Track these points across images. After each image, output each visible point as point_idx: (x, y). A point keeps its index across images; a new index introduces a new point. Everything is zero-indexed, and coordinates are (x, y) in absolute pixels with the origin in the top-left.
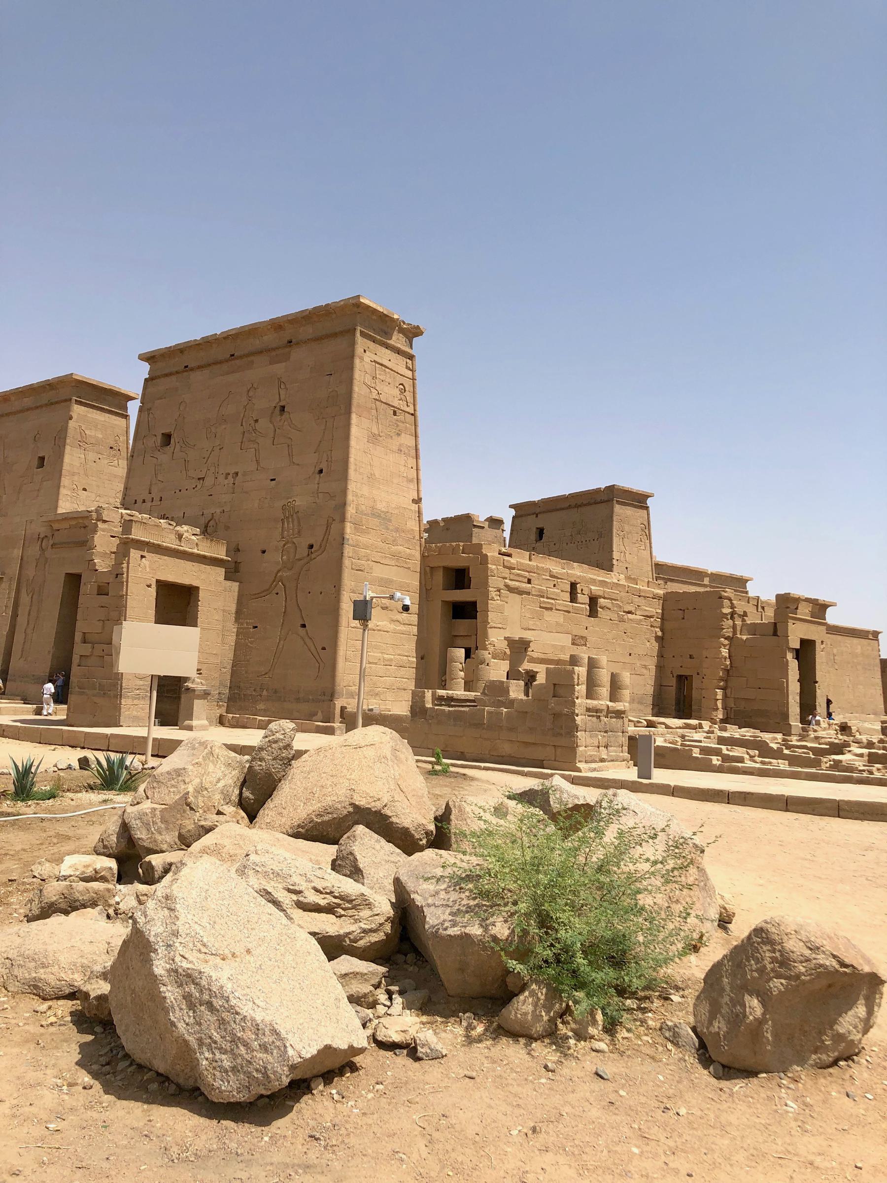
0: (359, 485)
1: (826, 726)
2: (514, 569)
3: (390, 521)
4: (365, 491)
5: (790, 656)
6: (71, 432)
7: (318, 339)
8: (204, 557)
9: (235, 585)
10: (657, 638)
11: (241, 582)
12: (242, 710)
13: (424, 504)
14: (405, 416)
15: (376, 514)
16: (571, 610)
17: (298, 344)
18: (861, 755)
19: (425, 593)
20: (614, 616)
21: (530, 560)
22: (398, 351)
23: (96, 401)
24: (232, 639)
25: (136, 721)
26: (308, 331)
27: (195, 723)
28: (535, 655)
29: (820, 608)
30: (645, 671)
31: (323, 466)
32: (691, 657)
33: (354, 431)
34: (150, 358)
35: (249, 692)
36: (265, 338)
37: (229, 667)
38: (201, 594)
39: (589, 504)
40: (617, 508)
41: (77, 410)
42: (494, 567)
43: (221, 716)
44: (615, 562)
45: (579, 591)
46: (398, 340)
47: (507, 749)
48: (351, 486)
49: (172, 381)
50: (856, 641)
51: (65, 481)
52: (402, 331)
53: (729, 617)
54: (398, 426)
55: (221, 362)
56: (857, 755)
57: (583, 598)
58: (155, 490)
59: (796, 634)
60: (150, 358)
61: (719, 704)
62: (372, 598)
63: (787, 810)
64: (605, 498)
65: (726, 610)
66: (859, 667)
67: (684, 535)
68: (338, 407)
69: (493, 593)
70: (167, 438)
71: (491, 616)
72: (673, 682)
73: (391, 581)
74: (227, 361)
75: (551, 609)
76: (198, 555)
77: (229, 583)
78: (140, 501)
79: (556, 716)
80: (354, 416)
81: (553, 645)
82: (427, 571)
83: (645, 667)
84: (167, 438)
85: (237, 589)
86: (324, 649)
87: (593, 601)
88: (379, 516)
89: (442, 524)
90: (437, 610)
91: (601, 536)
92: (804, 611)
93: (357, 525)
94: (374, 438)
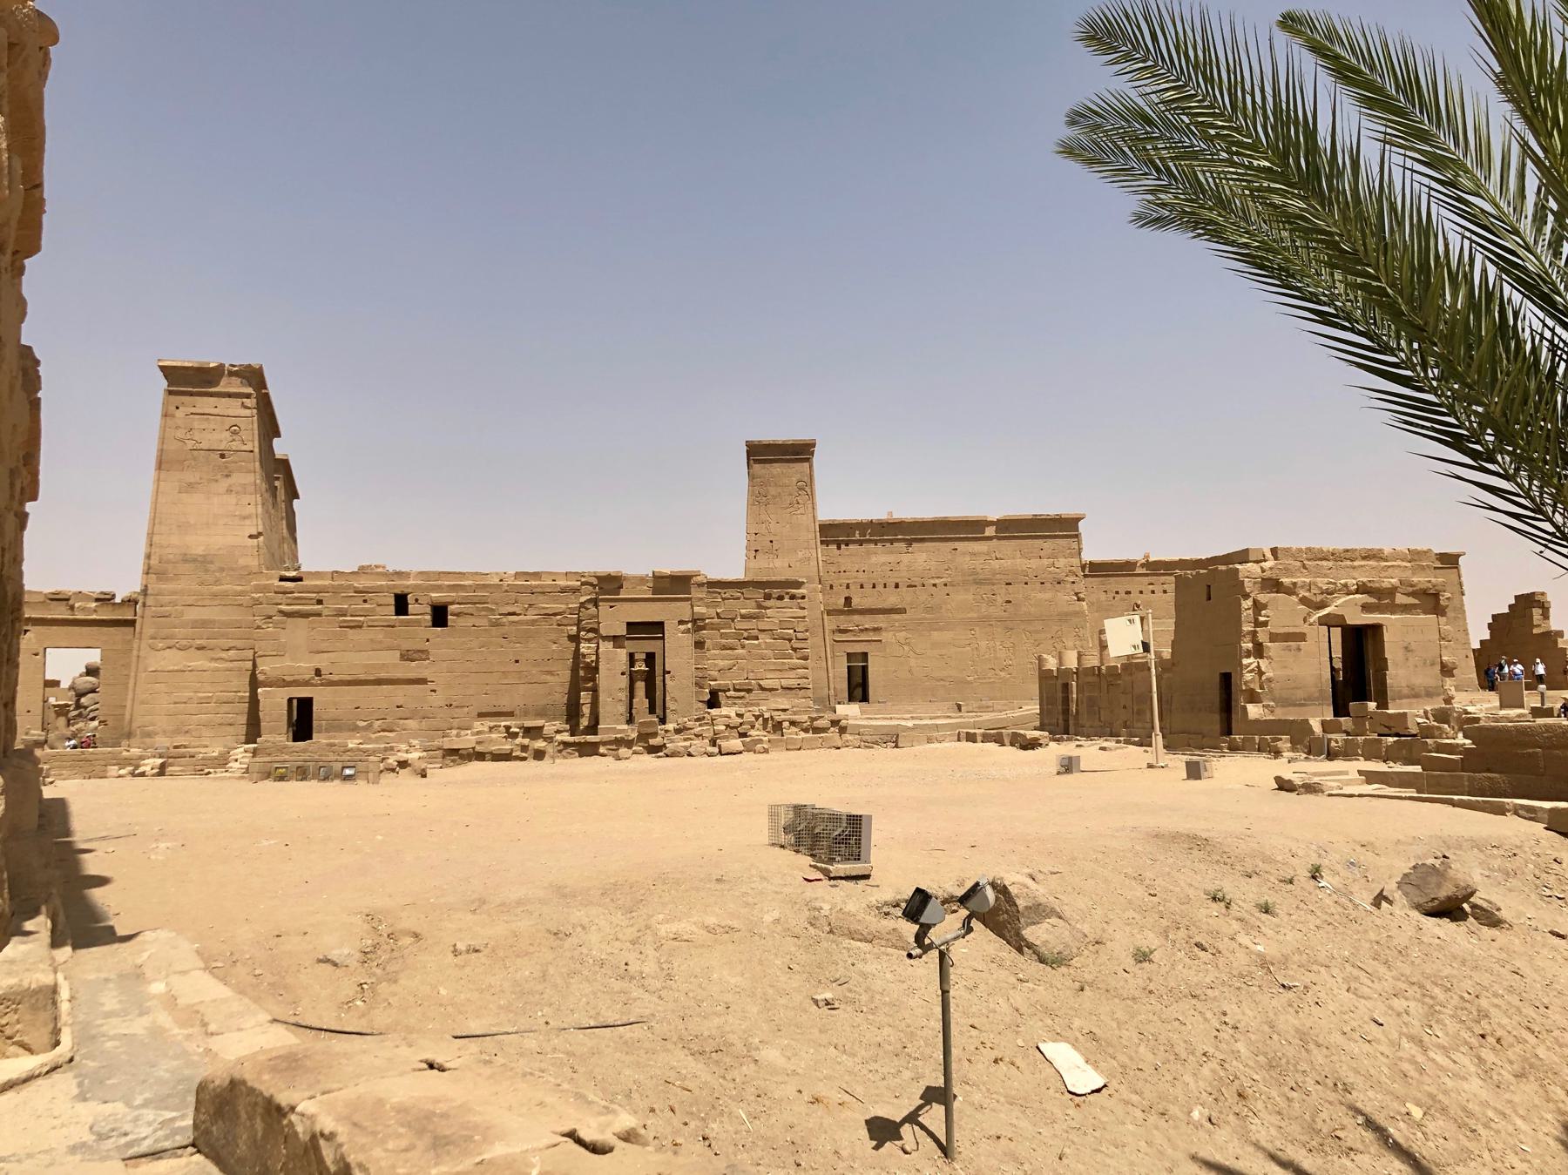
15: (186, 559)
22: (229, 395)
28: (335, 678)
30: (549, 678)
52: (231, 374)
57: (419, 611)
83: (550, 673)
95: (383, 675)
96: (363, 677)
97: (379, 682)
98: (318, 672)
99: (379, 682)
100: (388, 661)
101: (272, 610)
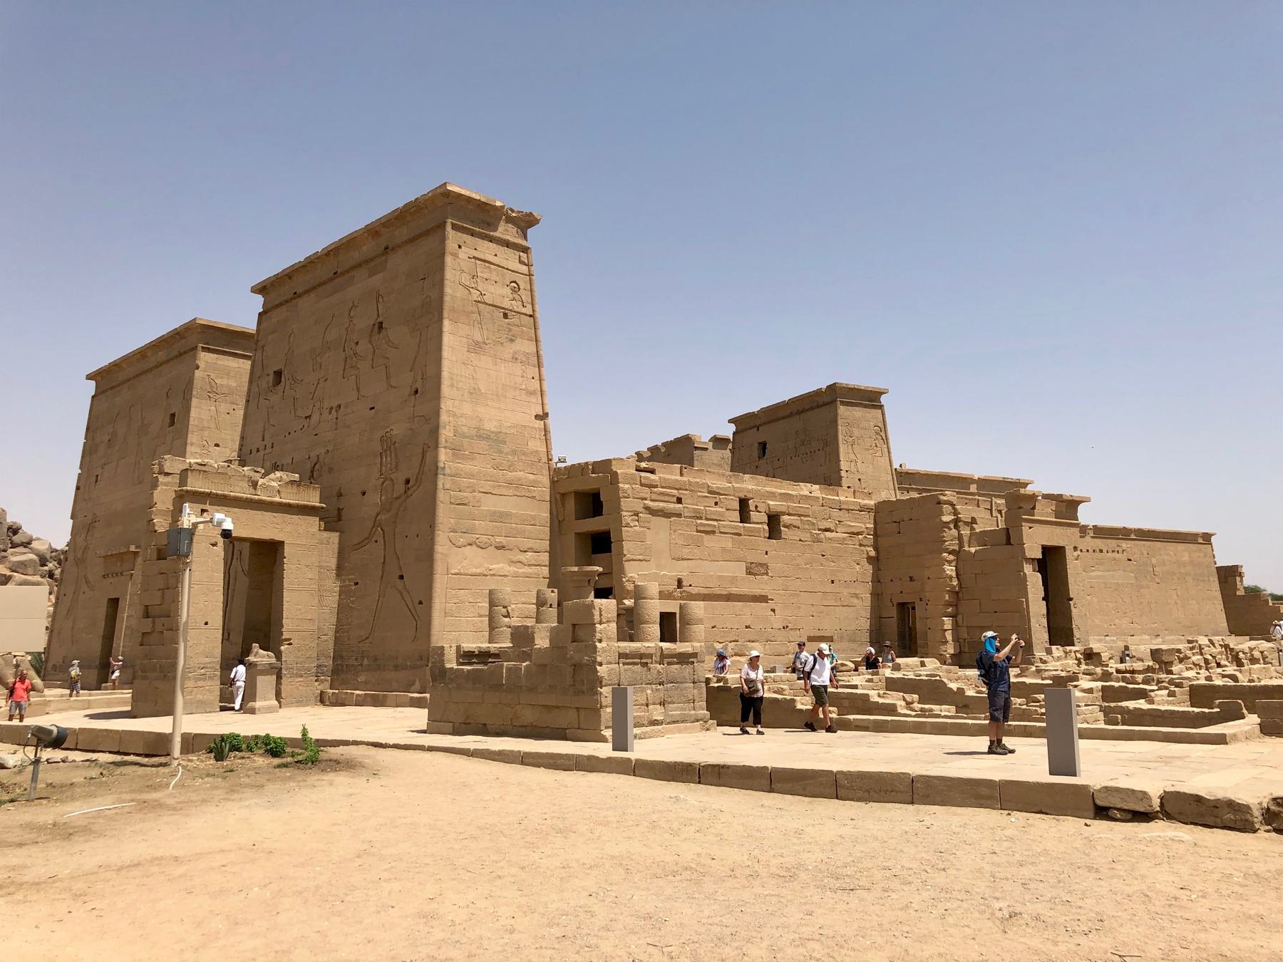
0: (457, 403)
1: (1062, 654)
2: (656, 486)
3: (505, 443)
4: (467, 408)
5: (1028, 569)
7: (412, 240)
8: (289, 505)
9: (335, 537)
10: (870, 559)
11: (342, 532)
12: (345, 684)
13: (550, 421)
14: (518, 320)
15: (482, 435)
16: (742, 532)
17: (393, 249)
18: (1090, 691)
20: (806, 536)
21: (681, 475)
22: (508, 244)
23: (227, 346)
24: (332, 600)
25: (198, 707)
26: (403, 233)
27: (258, 704)
28: (694, 590)
29: (1067, 507)
30: (855, 601)
31: (419, 385)
32: (911, 579)
33: (447, 339)
34: (261, 289)
35: (351, 662)
36: (364, 248)
37: (331, 634)
38: (287, 550)
39: (812, 408)
40: (842, 410)
41: (204, 358)
42: (627, 486)
43: (322, 692)
44: (843, 473)
45: (752, 508)
46: (505, 231)
47: (528, 716)
48: (446, 405)
49: (282, 313)
50: (1181, 547)
51: (192, 438)
52: (510, 220)
53: (952, 526)
54: (510, 330)
55: (324, 283)
56: (1084, 691)
57: (759, 517)
58: (267, 437)
59: (1034, 540)
60: (261, 289)
61: (949, 636)
62: (195, 525)
63: (771, 791)
64: (827, 399)
65: (947, 518)
66: (1189, 579)
67: (934, 433)
68: (428, 314)
69: (627, 517)
70: (278, 374)
71: (627, 546)
72: (894, 612)
73: (508, 515)
74: (331, 280)
75: (713, 532)
76: (280, 504)
77: (326, 534)
78: (254, 451)
79: (577, 667)
80: (446, 323)
81: (720, 578)
83: (856, 596)
84: (278, 374)
85: (337, 540)
86: (421, 603)
87: (774, 520)
88: (488, 438)
89: (663, 450)
91: (826, 444)
92: (1044, 511)
93: (456, 451)
95: (734, 590)
96: (717, 591)
97: (729, 598)
98: (680, 583)
99: (729, 598)
100: (729, 573)
101: (639, 506)
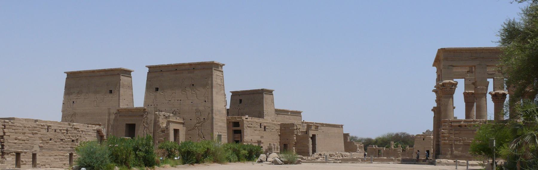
6: (121, 84)
19: (228, 128)
34: (150, 67)
40: (265, 95)
41: (122, 77)
46: (220, 67)
57: (263, 127)
59: (311, 133)
71: (245, 134)
82: (229, 122)
87: (265, 127)
90: (231, 132)
94: (217, 93)
